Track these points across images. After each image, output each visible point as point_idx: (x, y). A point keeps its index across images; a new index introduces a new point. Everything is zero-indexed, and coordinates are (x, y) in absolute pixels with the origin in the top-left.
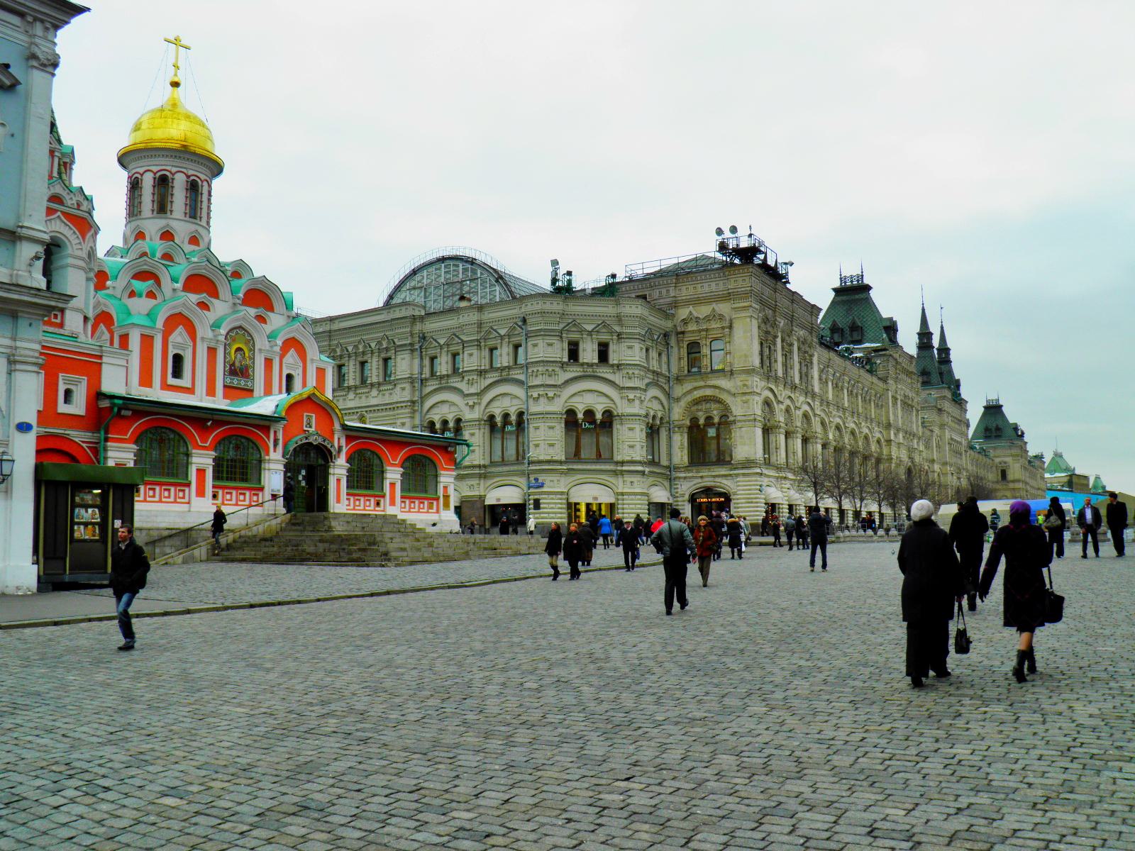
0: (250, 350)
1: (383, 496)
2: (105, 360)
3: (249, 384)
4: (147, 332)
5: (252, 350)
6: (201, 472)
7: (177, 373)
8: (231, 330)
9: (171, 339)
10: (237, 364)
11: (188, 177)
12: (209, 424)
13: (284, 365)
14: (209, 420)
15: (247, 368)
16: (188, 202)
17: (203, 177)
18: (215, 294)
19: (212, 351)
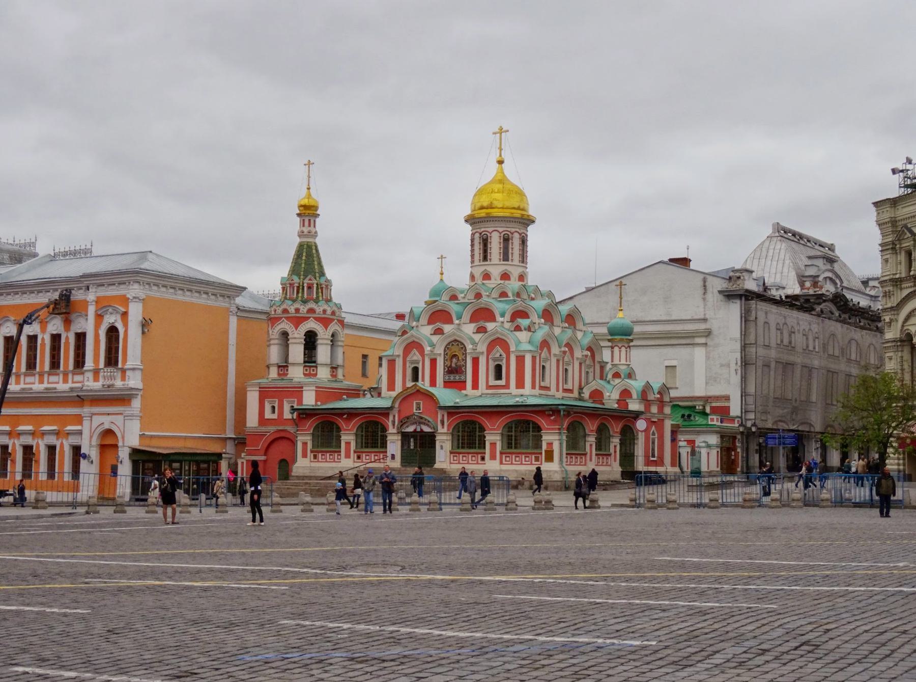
0: (463, 354)
1: (485, 453)
2: (304, 388)
3: (463, 378)
4: (390, 358)
5: (465, 354)
6: (348, 444)
7: (415, 378)
8: (449, 344)
9: (408, 359)
10: (453, 365)
11: (480, 234)
12: (345, 416)
13: (490, 361)
14: (344, 414)
15: (460, 367)
16: (481, 252)
17: (490, 230)
18: (449, 321)
19: (433, 362)
